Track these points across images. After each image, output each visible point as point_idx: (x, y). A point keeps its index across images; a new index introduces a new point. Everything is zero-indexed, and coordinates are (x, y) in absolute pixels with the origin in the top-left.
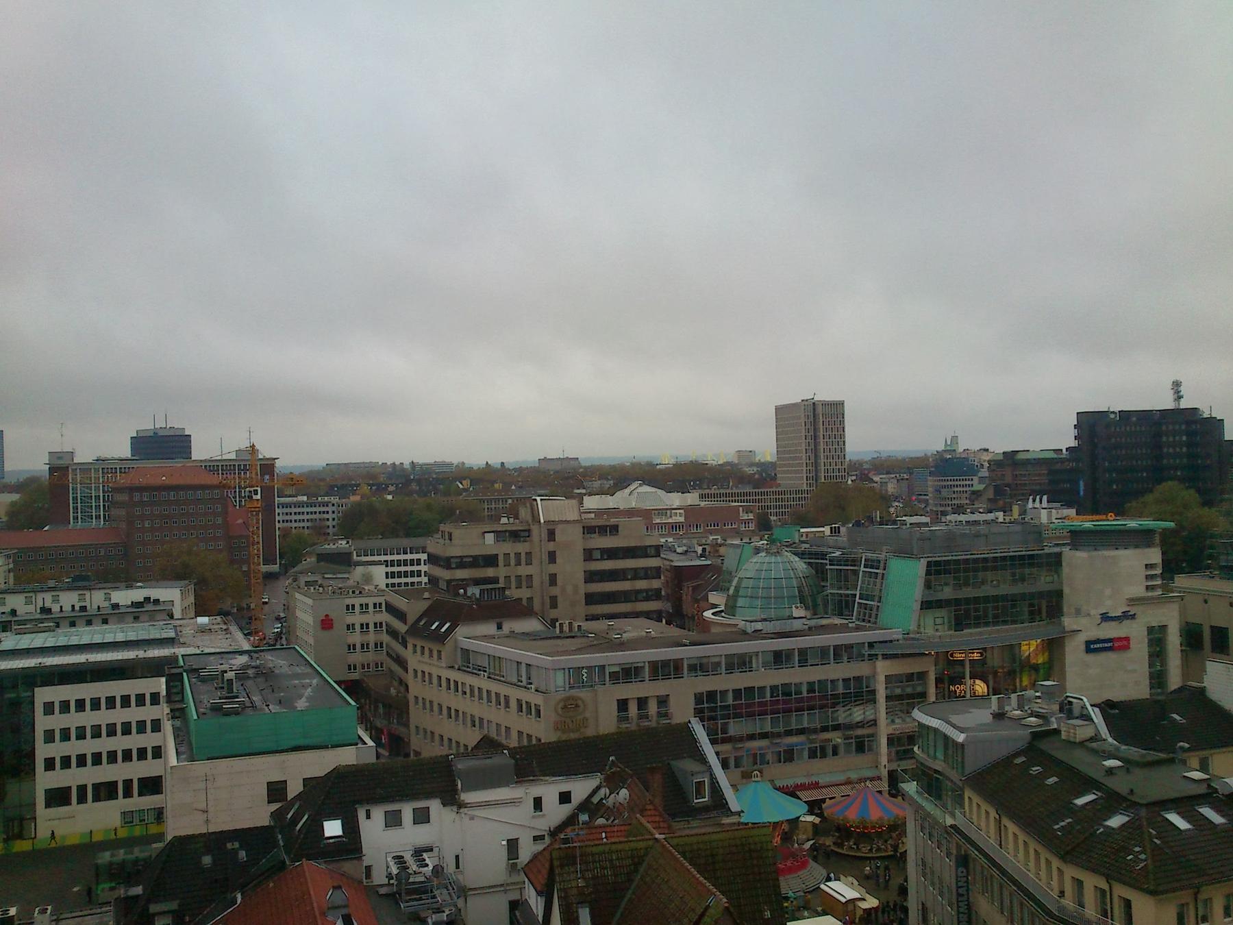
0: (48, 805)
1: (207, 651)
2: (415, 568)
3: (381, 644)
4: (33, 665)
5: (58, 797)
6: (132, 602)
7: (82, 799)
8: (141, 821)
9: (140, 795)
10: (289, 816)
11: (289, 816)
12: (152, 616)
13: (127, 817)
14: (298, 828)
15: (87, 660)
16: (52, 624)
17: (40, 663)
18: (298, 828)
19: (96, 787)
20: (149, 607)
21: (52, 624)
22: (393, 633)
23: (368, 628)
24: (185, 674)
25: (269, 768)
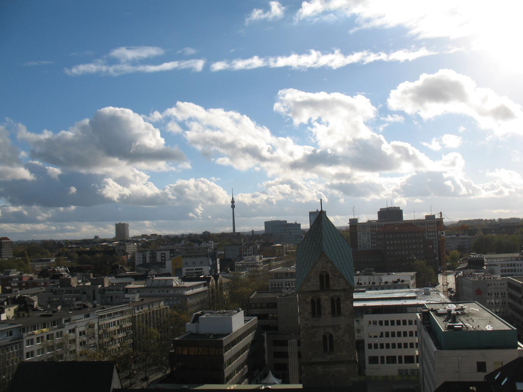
0: (370, 363)
1: (431, 302)
2: (513, 268)
3: (505, 303)
4: (362, 305)
5: (374, 360)
6: (393, 281)
7: (382, 362)
8: (406, 374)
9: (405, 363)
10: (496, 378)
11: (496, 378)
12: (401, 287)
13: (401, 372)
14: (503, 384)
15: (383, 304)
16: (364, 289)
17: (365, 305)
18: (503, 384)
19: (388, 357)
20: (399, 283)
21: (364, 289)
22: (511, 296)
23: (498, 295)
24: (430, 312)
25: (478, 355)
